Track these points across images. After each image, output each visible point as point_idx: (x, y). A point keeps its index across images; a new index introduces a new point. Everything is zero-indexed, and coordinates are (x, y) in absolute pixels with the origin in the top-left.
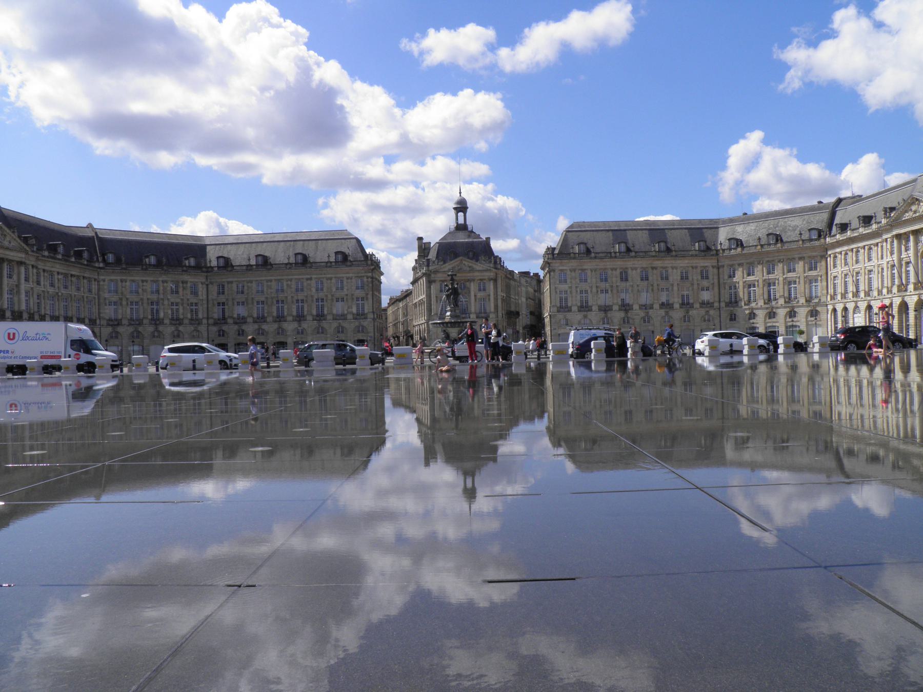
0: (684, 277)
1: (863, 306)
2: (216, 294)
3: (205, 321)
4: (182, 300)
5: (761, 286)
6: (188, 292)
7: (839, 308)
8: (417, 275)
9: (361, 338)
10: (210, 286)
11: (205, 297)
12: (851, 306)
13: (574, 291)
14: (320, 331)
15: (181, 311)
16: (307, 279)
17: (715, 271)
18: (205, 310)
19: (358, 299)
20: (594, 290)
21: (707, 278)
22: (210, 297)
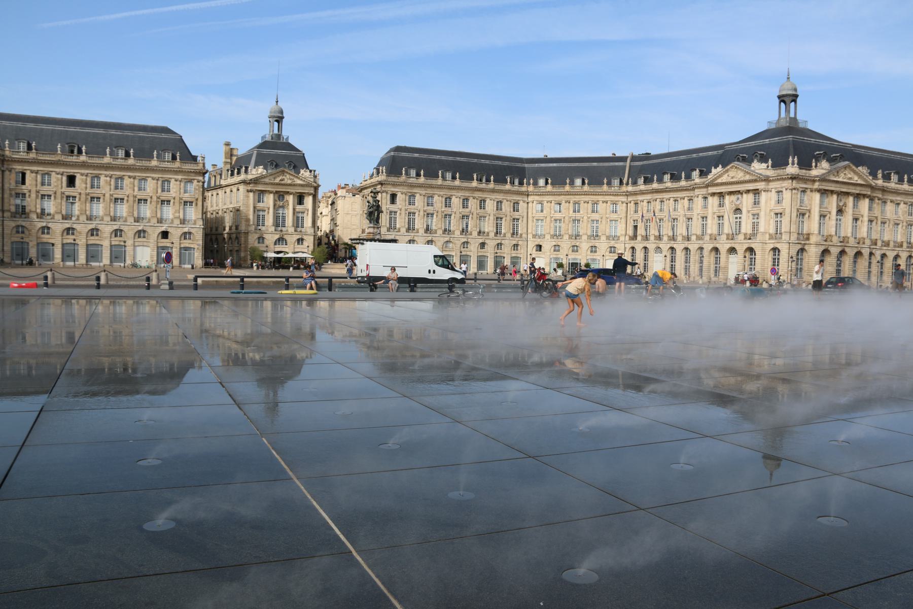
0: (499, 208)
1: (665, 247)
5: (567, 222)
7: (639, 247)
9: (187, 245)
12: (651, 246)
13: (403, 212)
14: (141, 233)
17: (525, 205)
19: (185, 202)
20: (422, 213)
21: (518, 211)
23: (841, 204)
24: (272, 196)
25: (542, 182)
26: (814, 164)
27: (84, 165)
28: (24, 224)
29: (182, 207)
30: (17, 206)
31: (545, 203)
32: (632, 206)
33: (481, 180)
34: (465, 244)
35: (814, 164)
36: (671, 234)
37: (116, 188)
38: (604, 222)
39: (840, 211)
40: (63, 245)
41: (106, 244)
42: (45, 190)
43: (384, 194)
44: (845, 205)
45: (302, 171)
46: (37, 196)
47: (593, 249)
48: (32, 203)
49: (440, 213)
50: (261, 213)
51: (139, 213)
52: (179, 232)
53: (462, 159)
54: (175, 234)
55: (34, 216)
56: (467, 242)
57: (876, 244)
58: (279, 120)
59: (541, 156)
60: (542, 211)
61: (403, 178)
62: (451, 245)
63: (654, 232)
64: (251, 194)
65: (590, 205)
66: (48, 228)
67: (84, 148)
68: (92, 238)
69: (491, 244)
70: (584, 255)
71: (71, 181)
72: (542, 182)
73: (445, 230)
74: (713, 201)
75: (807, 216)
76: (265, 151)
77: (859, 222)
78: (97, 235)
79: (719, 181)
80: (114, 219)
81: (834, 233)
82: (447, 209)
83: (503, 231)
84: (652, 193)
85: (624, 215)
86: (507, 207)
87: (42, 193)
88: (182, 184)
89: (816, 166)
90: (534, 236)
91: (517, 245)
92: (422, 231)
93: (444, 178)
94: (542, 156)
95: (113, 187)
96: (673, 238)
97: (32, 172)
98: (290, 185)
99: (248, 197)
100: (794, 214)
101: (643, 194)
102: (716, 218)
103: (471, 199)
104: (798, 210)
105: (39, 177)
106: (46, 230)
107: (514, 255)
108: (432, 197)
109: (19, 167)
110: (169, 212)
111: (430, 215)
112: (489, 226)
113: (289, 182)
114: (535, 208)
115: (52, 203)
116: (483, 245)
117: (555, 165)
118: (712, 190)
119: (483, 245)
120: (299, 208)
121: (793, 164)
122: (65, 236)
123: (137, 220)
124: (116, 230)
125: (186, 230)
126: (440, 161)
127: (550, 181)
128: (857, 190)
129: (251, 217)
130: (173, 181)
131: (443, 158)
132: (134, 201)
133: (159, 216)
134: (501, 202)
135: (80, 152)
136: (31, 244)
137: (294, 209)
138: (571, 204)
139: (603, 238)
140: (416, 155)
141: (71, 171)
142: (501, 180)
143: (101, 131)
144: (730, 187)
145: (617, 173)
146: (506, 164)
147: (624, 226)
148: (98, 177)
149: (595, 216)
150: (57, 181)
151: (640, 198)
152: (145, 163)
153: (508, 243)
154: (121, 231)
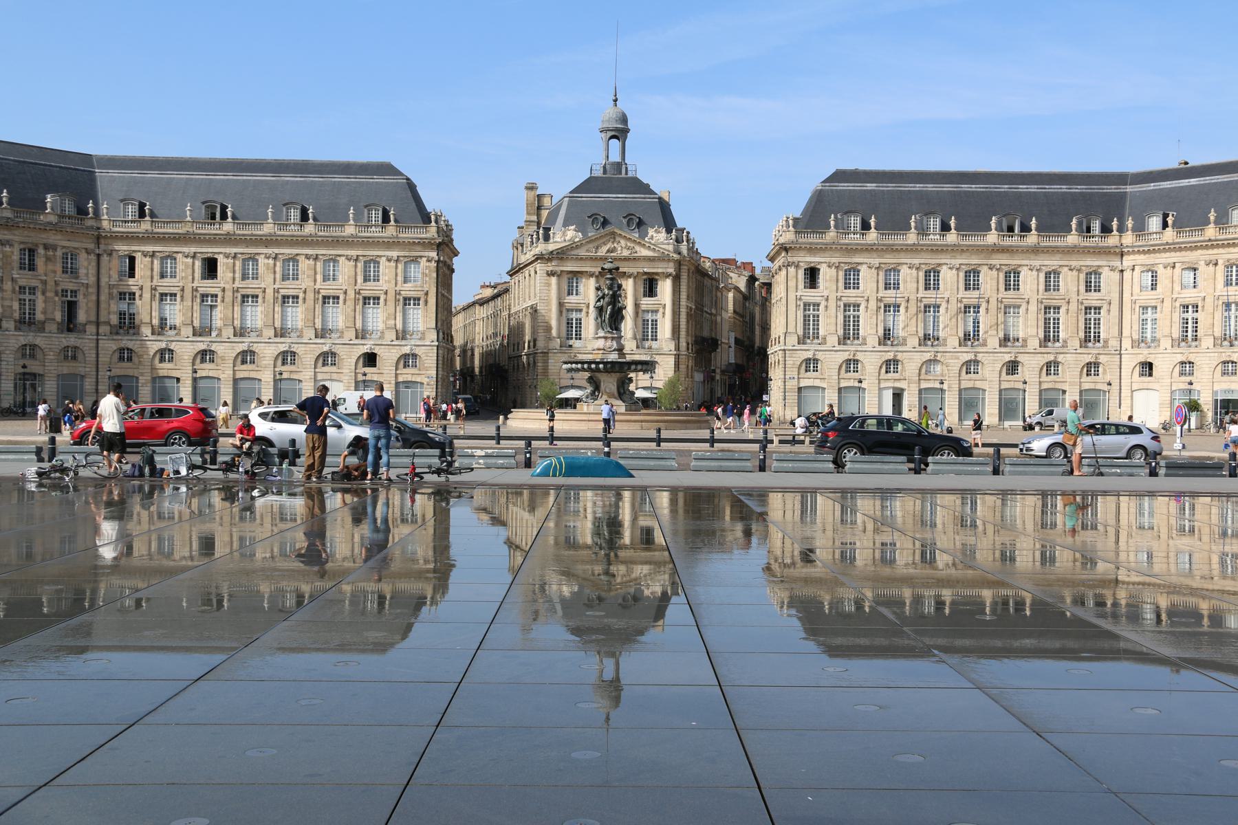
2: (115, 276)
3: (91, 329)
4: (45, 283)
6: (59, 267)
8: (523, 259)
9: (409, 378)
10: (105, 258)
11: (92, 279)
13: (832, 304)
15: (40, 305)
16: (308, 257)
17: (1116, 275)
18: (93, 305)
19: (406, 300)
20: (873, 304)
22: (104, 280)
24: (592, 281)
27: (229, 240)
28: (130, 345)
29: (399, 308)
30: (122, 314)
31: (1160, 270)
33: (1011, 229)
34: (971, 366)
37: (285, 278)
40: (195, 380)
41: (267, 377)
42: (167, 285)
43: (792, 270)
45: (651, 232)
46: (153, 297)
48: (145, 309)
49: (912, 304)
50: (574, 315)
51: (324, 321)
52: (395, 354)
53: (974, 188)
54: (388, 357)
55: (146, 331)
56: (976, 362)
58: (620, 133)
59: (1173, 164)
60: (1154, 286)
61: (831, 235)
62: (938, 368)
64: (554, 280)
66: (171, 351)
67: (229, 211)
68: (244, 367)
69: (1031, 365)
71: (210, 268)
72: (1154, 223)
73: (926, 337)
76: (585, 197)
78: (253, 362)
80: (281, 333)
86: (1070, 283)
87: (161, 290)
88: (400, 266)
90: (1136, 344)
91: (1097, 365)
92: (872, 341)
93: (923, 231)
94: (1175, 165)
95: (278, 276)
97: (145, 255)
98: (626, 259)
99: (549, 285)
103: (984, 270)
105: (156, 263)
106: (166, 354)
107: (1086, 386)
108: (896, 270)
109: (123, 248)
110: (378, 318)
111: (891, 308)
112: (1027, 326)
113: (626, 253)
114: (1136, 281)
115: (178, 307)
116: (1012, 367)
117: (1193, 181)
119: (1012, 367)
120: (646, 302)
122: (240, 367)
123: (322, 333)
124: (284, 353)
125: (406, 350)
126: (921, 195)
127: (1170, 220)
129: (554, 323)
130: (383, 261)
132: (316, 300)
133: (359, 325)
134: (1056, 273)
135: (224, 216)
136: (142, 380)
137: (637, 306)
138: (1221, 267)
140: (871, 186)
141: (209, 250)
142: (1054, 225)
143: (268, 178)
146: (1078, 189)
148: (253, 258)
150: (187, 269)
152: (335, 232)
153: (1072, 360)
154: (294, 354)
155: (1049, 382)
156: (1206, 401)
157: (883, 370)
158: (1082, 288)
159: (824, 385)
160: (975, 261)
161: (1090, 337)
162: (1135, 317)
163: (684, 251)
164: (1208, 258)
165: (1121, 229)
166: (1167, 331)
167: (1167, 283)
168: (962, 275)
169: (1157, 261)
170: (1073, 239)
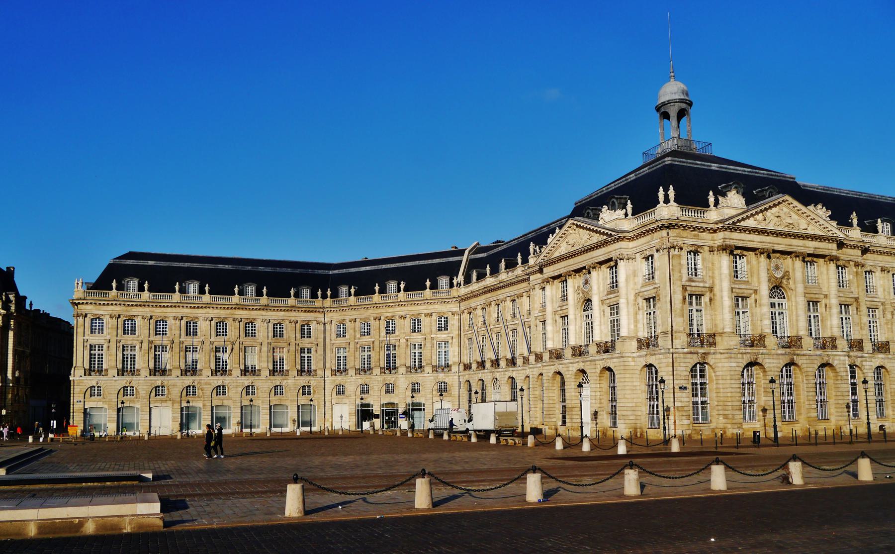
13: (113, 345)
17: (321, 327)
20: (145, 346)
23: (779, 275)
25: (344, 290)
26: (711, 199)
32: (466, 316)
35: (711, 199)
36: (509, 356)
38: (428, 345)
39: (777, 288)
43: (81, 319)
44: (786, 275)
47: (416, 389)
57: (861, 349)
59: (359, 259)
61: (114, 293)
63: (490, 355)
65: (408, 320)
70: (402, 396)
74: (553, 291)
75: (705, 299)
77: (821, 308)
79: (557, 254)
81: (768, 330)
82: (189, 338)
83: (285, 367)
84: (485, 293)
85: (456, 333)
86: (290, 332)
89: (716, 203)
90: (335, 373)
93: (183, 291)
96: (512, 362)
100: (678, 297)
101: (476, 296)
102: (560, 320)
104: (684, 288)
117: (368, 268)
118: (549, 271)
121: (667, 201)
127: (353, 290)
128: (810, 246)
131: (195, 265)
139: (428, 369)
140: (151, 263)
144: (571, 261)
145: (451, 270)
146: (298, 271)
147: (457, 349)
149: (417, 338)
151: (473, 303)
155: (275, 400)
156: (377, 410)
157: (153, 394)
158: (299, 335)
159: (106, 406)
160: (222, 313)
161: (304, 370)
162: (333, 355)
163: (13, 309)
164: (375, 315)
165: (324, 297)
166: (352, 364)
167: (352, 332)
168: (213, 323)
169: (346, 318)
170: (292, 301)
